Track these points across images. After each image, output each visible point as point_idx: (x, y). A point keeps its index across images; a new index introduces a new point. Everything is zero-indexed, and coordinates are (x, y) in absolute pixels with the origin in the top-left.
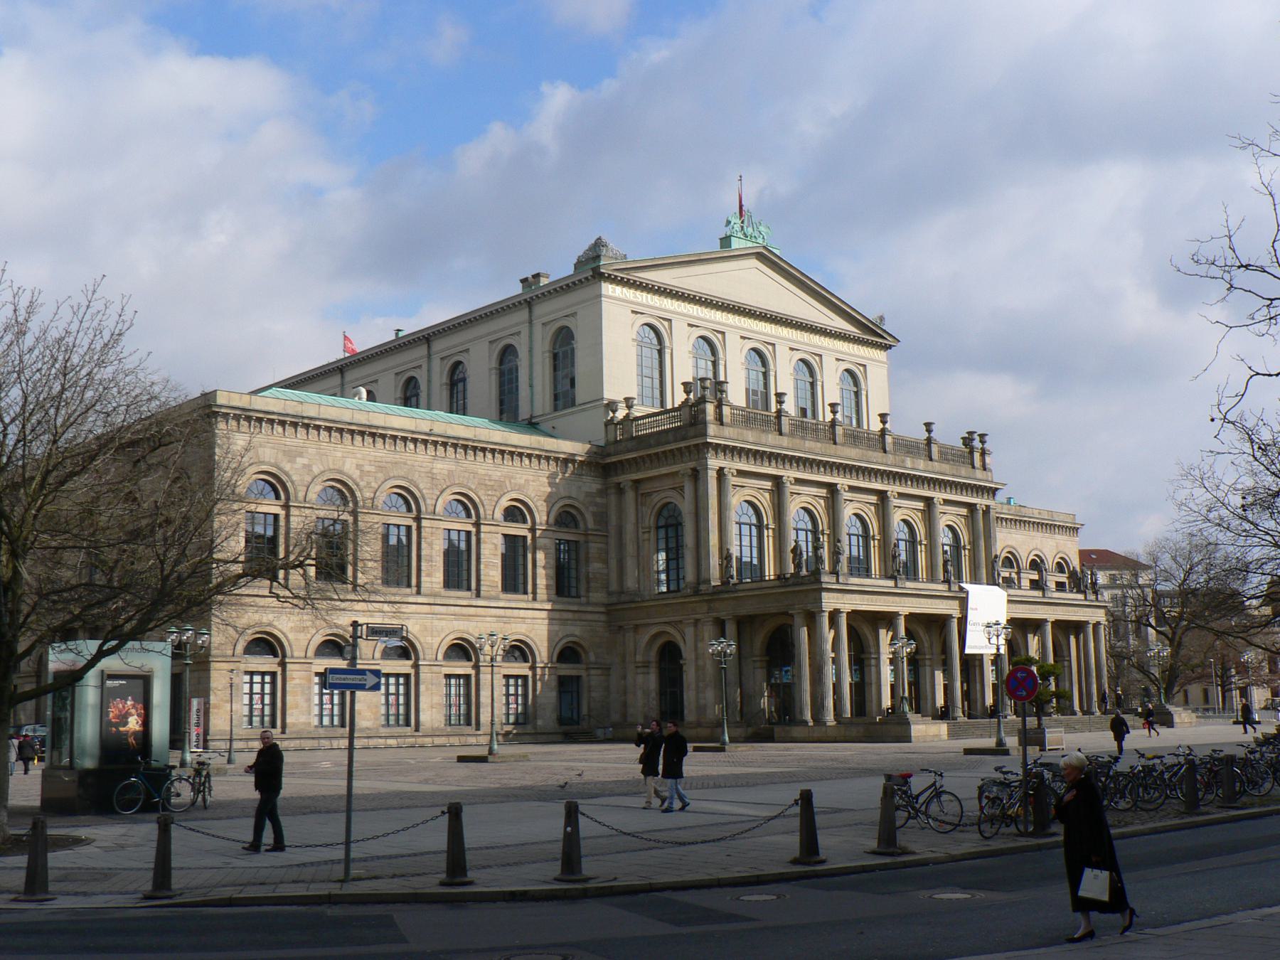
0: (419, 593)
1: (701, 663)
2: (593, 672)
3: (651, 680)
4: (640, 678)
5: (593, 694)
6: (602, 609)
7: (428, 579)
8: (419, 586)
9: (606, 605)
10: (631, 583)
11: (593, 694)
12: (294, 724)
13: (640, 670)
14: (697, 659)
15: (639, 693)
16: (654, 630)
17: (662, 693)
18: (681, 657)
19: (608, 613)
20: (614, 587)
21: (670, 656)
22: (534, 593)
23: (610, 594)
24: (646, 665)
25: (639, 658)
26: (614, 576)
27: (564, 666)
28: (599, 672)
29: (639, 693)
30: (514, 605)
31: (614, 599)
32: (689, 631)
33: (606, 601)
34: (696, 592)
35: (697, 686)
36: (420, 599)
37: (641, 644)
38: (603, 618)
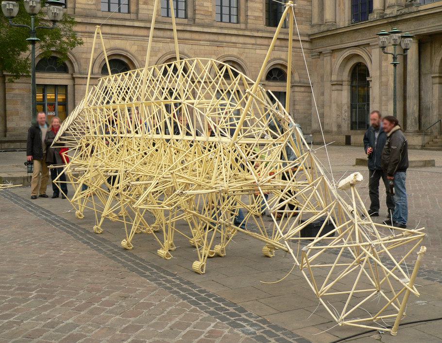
0: (137, 20)
1: (384, 79)
2: (297, 89)
3: (344, 96)
4: (335, 94)
5: (297, 107)
6: (306, 39)
7: (145, 6)
8: (137, 13)
9: (309, 35)
10: (328, 16)
11: (297, 107)
12: (14, 129)
13: (334, 88)
14: (381, 76)
15: (334, 106)
16: (347, 53)
17: (352, 107)
18: (368, 75)
19: (311, 41)
20: (315, 20)
21: (360, 75)
22: (246, 23)
23: (312, 26)
24: (340, 84)
25: (334, 78)
26: (316, 11)
27: (271, 83)
28: (302, 89)
29: (334, 106)
30: (226, 31)
31: (316, 30)
32: (376, 52)
33: (310, 33)
34: (383, 17)
35: (381, 100)
36: (136, 24)
37: (336, 67)
38: (307, 45)
